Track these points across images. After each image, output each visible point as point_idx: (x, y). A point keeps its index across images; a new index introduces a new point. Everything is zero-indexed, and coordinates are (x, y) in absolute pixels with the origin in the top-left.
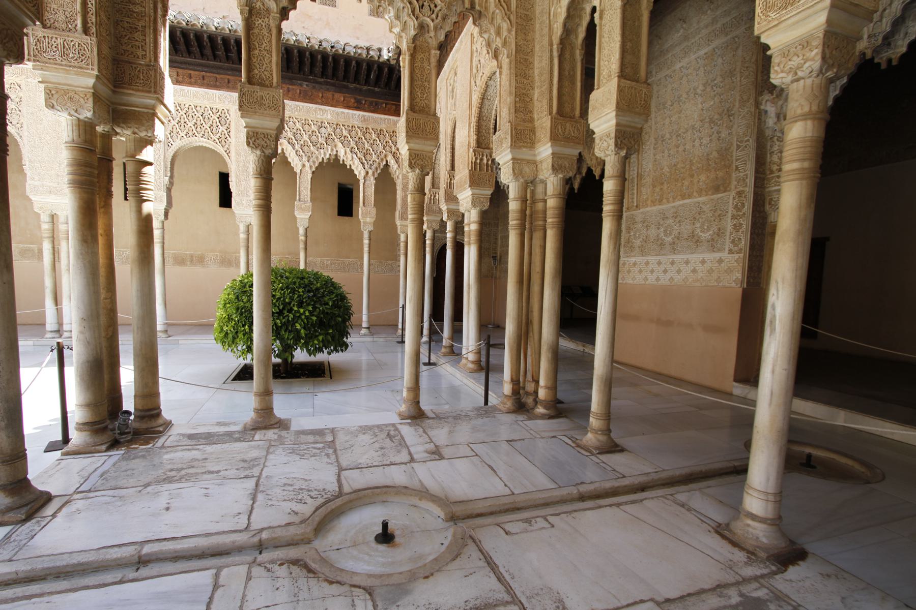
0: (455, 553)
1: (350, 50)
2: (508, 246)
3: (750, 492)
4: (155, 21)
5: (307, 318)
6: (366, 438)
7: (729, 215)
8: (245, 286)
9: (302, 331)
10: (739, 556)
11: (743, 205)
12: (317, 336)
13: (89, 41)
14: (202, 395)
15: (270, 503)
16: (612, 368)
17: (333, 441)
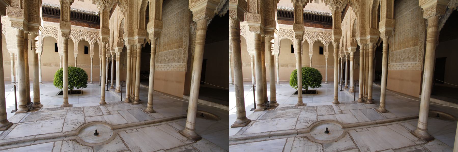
0: (114, 138)
1: (88, 12)
2: (127, 61)
3: (188, 122)
4: (39, 5)
5: (77, 79)
6: (92, 109)
7: (182, 54)
8: (61, 71)
9: (76, 83)
10: (185, 139)
11: (186, 51)
12: (79, 84)
13: (22, 10)
14: (50, 98)
15: (67, 125)
16: (153, 92)
17: (83, 110)
